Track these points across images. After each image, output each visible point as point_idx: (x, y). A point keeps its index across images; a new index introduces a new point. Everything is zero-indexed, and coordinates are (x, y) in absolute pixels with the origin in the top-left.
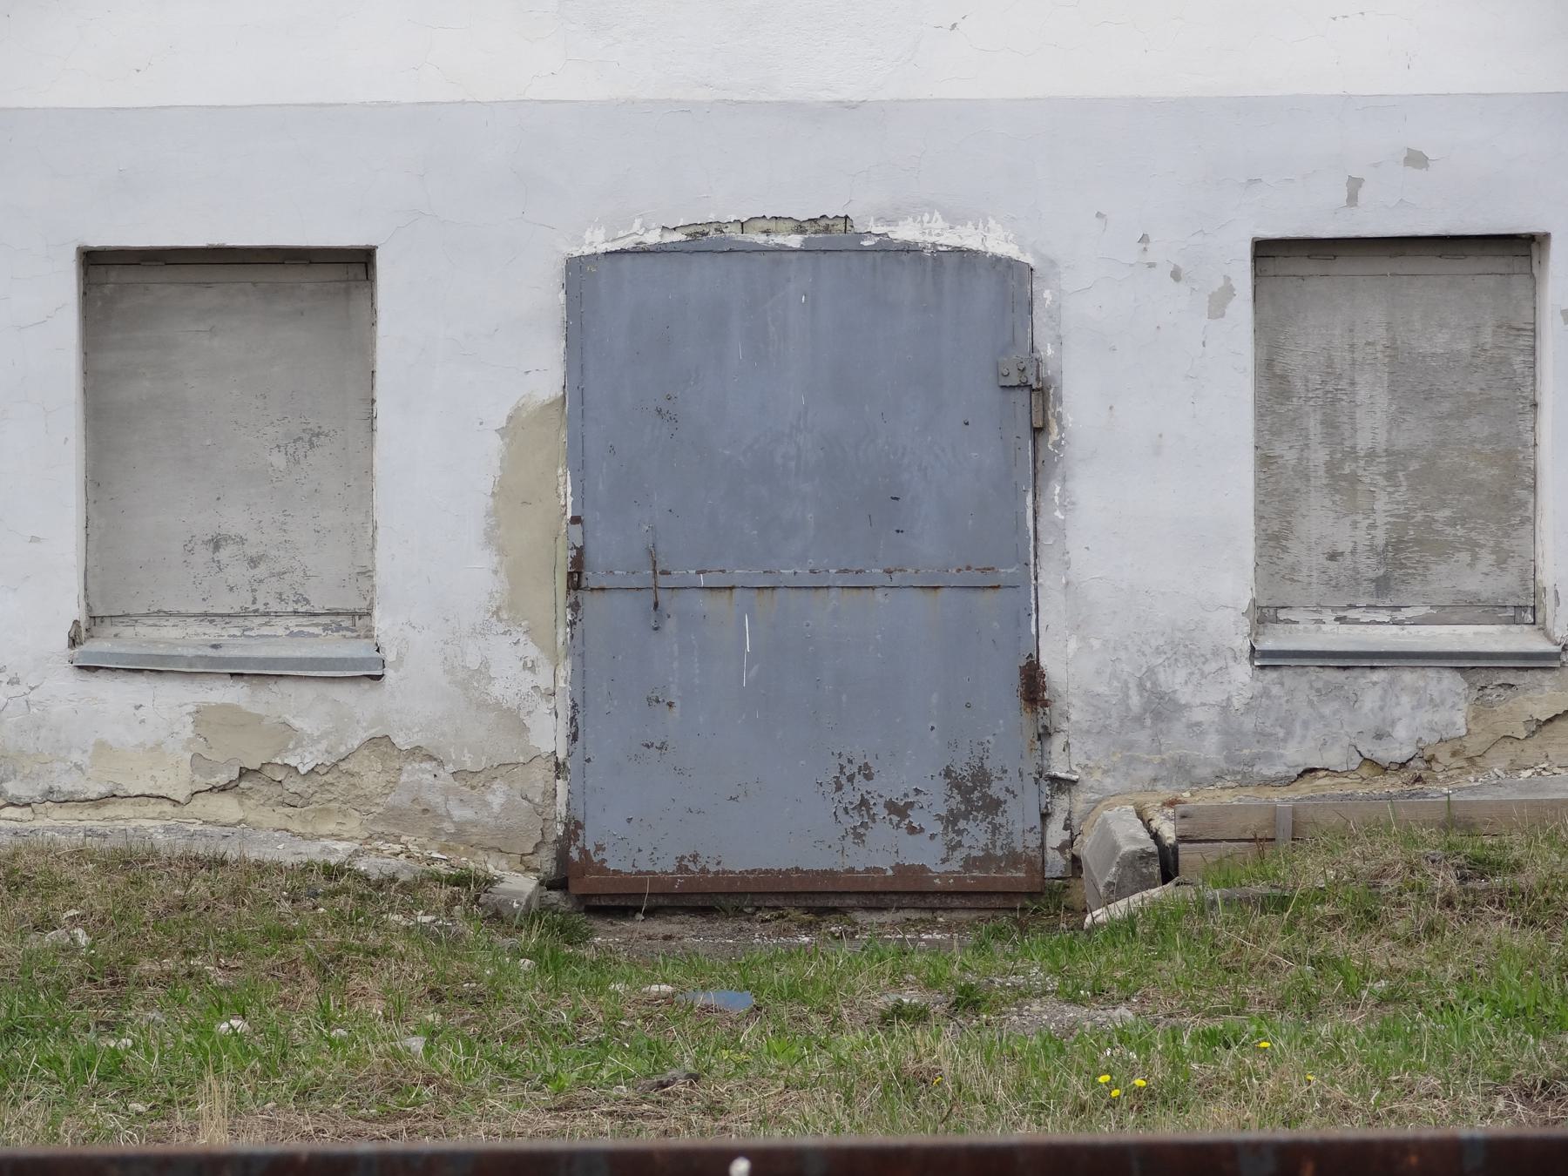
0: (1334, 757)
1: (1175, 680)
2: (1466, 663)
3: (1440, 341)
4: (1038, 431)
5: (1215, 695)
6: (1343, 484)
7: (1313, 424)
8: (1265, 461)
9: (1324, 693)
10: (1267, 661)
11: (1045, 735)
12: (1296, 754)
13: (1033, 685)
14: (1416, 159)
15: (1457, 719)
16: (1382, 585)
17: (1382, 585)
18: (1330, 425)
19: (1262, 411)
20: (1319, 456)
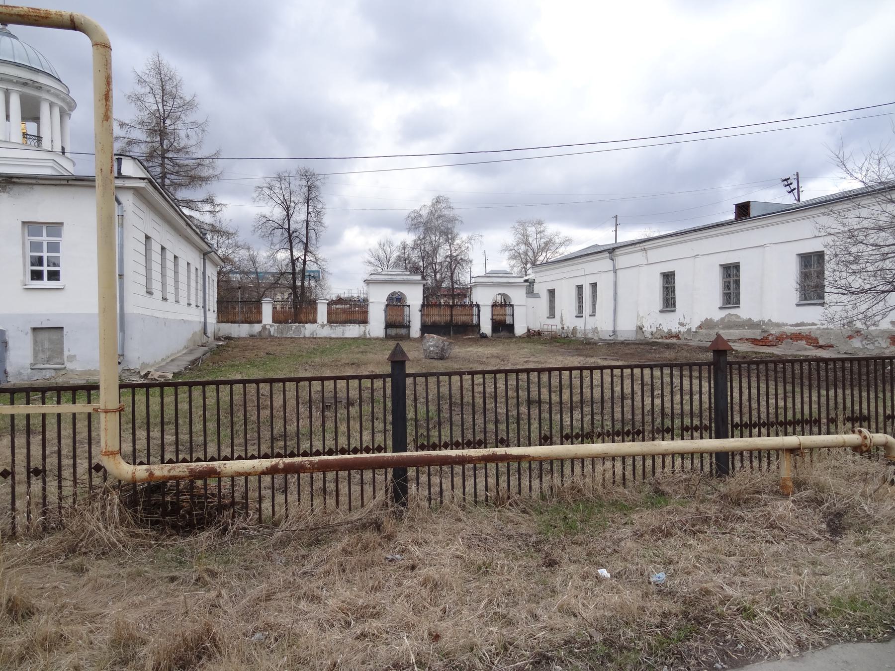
0: (40, 378)
1: (21, 371)
2: (55, 369)
3: (54, 337)
4: (6, 346)
5: (27, 372)
6: (43, 351)
7: (40, 346)
8: (34, 349)
9: (39, 372)
10: (32, 369)
11: (7, 376)
12: (36, 378)
13: (5, 372)
14: (48, 320)
15: (54, 374)
16: (48, 361)
17: (48, 361)
18: (42, 346)
19: (34, 344)
20: (41, 349)
